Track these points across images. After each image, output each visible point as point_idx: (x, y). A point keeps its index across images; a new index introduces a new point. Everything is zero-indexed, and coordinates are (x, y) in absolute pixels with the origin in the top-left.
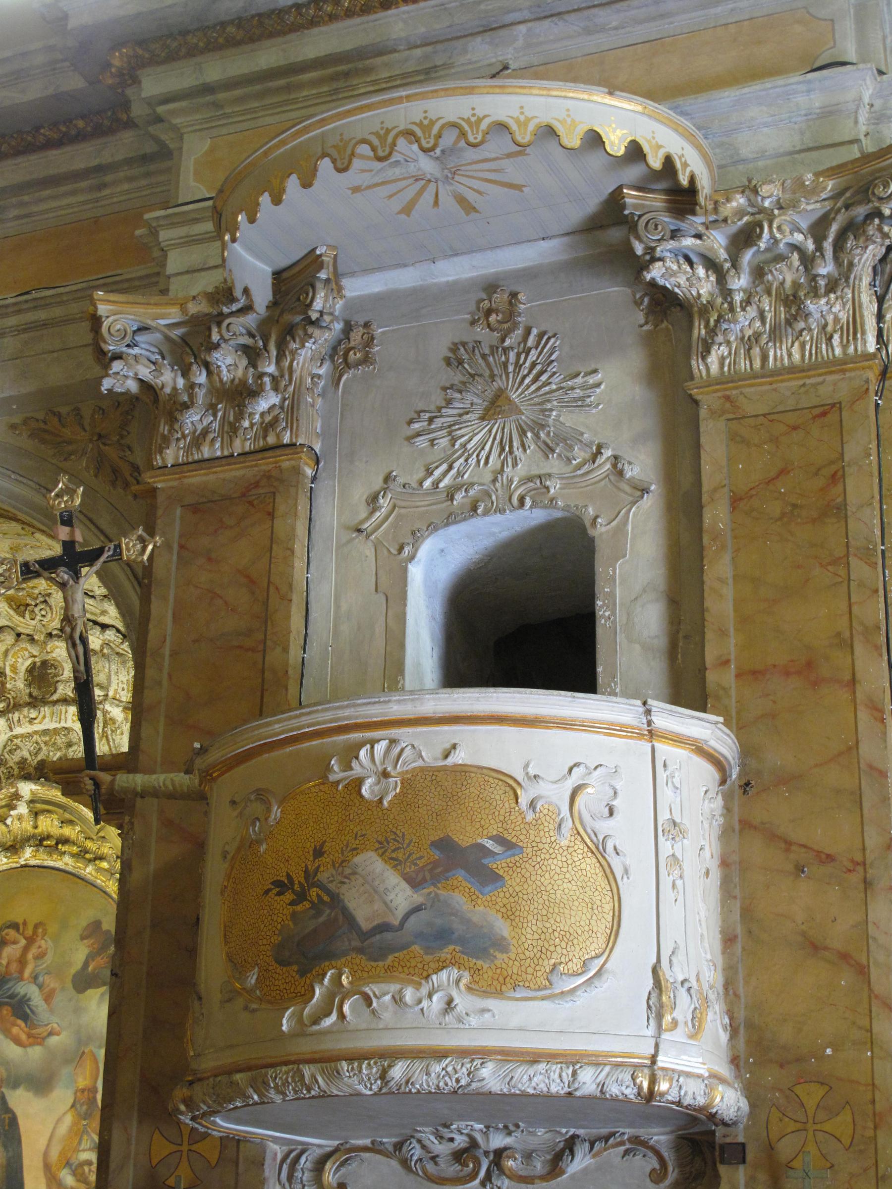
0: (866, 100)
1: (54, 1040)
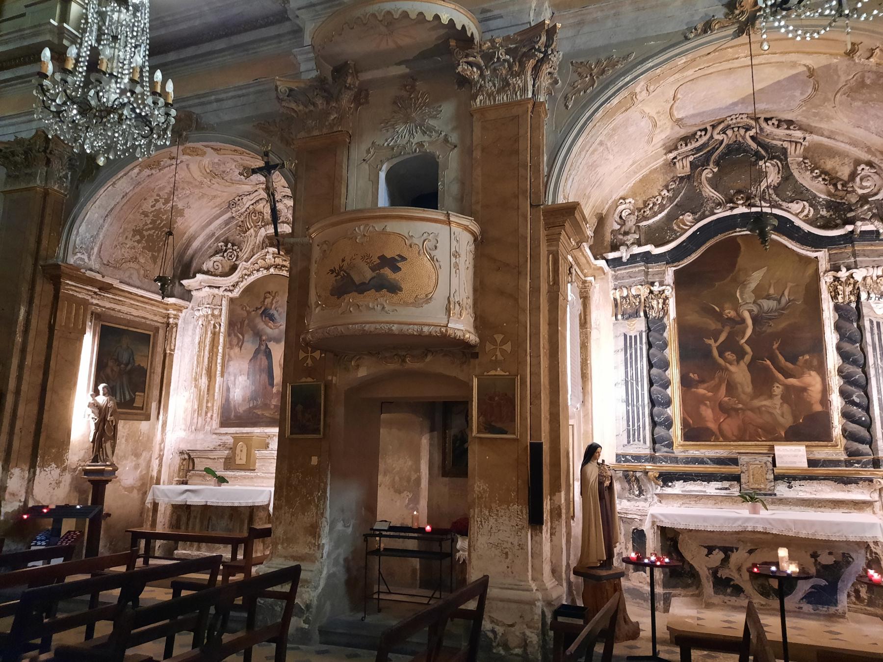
0: (533, 7)
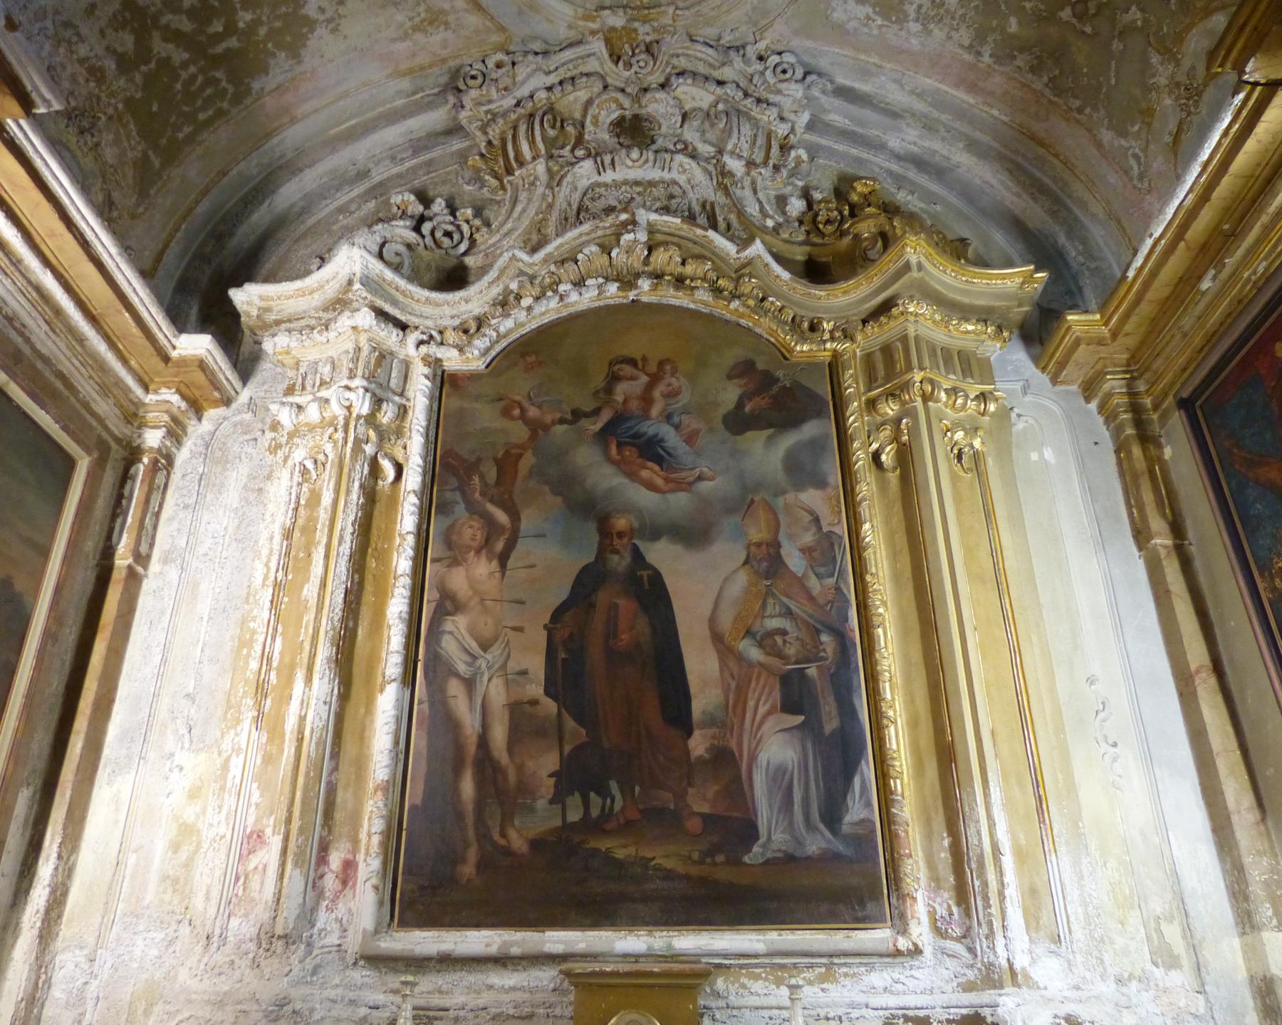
1: (704, 486)
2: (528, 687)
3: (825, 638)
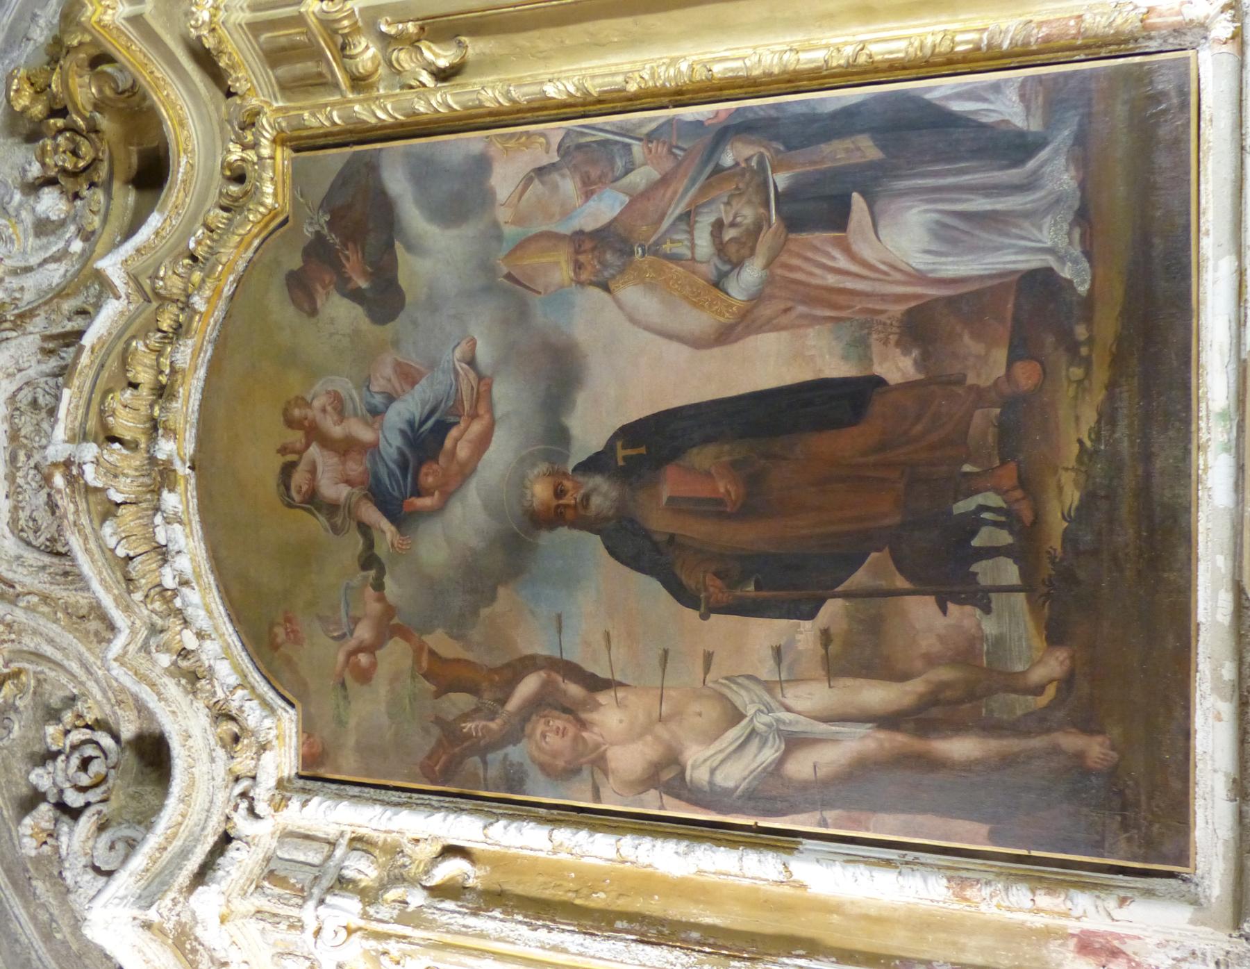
1: (484, 354)
2: (801, 646)
3: (728, 159)
